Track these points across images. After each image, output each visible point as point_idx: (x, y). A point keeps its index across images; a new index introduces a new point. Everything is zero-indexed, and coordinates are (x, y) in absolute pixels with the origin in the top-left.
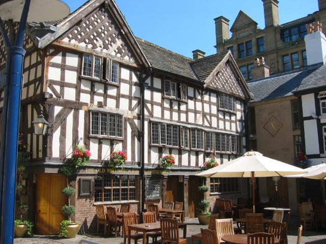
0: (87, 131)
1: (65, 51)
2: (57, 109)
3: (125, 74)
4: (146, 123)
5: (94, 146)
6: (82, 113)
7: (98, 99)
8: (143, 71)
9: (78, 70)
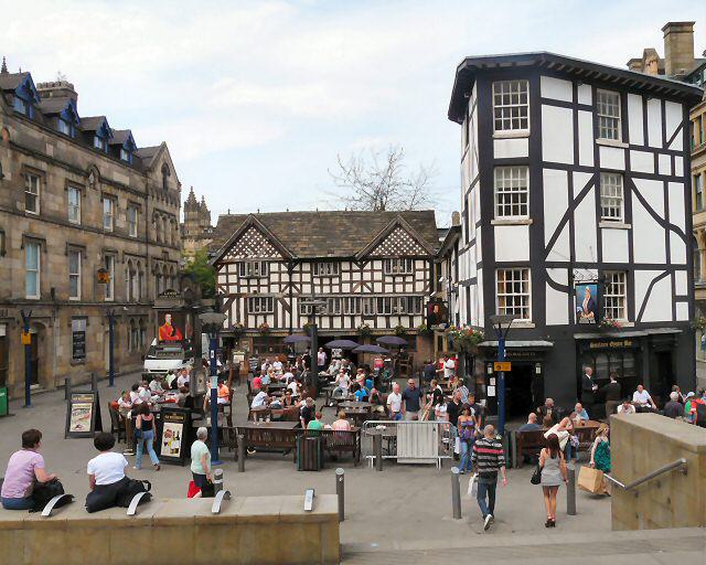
1: (227, 264)
2: (226, 300)
3: (274, 267)
4: (295, 300)
5: (251, 319)
6: (242, 300)
7: (252, 289)
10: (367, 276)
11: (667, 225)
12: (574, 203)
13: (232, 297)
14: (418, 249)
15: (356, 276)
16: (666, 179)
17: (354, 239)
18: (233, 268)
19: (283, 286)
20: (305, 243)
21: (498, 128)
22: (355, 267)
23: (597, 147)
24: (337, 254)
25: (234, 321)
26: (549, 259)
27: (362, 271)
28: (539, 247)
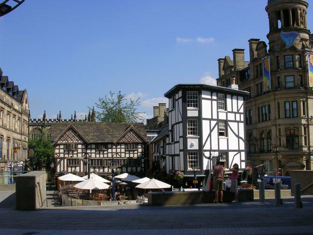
0: (67, 164)
1: (59, 145)
2: (58, 160)
3: (80, 146)
6: (66, 160)
7: (70, 155)
9: (64, 149)
10: (119, 150)
11: (238, 136)
12: (211, 131)
13: (61, 159)
14: (139, 141)
15: (114, 150)
16: (238, 122)
17: (112, 135)
18: (62, 147)
20: (92, 136)
21: (189, 106)
23: (218, 112)
24: (106, 141)
25: (62, 170)
26: (204, 149)
27: (116, 148)
28: (201, 145)
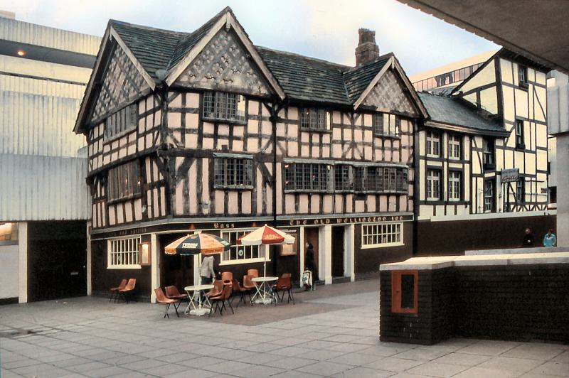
2: (180, 161)
4: (279, 165)
5: (219, 196)
6: (205, 162)
7: (222, 142)
8: (275, 101)
13: (190, 155)
15: (348, 133)
18: (193, 100)
19: (264, 142)
22: (347, 121)
